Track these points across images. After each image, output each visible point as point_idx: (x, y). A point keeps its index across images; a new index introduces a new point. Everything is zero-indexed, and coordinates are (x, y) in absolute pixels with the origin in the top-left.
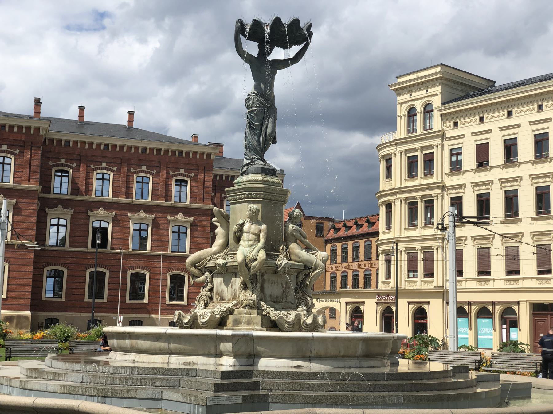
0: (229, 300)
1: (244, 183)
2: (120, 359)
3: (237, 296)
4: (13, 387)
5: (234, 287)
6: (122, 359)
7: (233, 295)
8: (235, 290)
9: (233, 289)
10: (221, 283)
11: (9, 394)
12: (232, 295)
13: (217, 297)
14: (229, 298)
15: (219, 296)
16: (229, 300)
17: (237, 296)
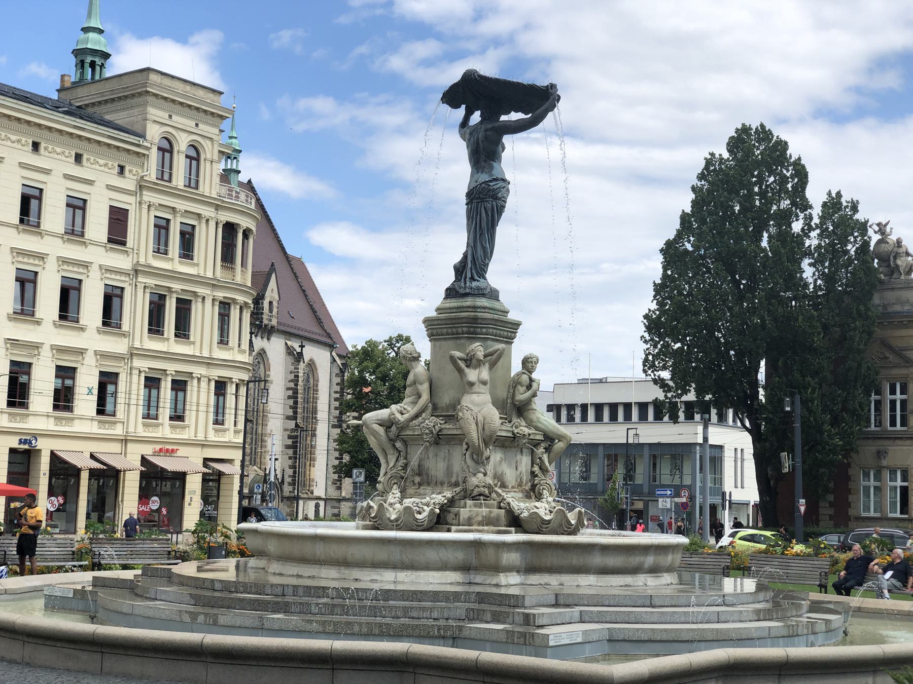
0: (513, 487)
1: (500, 313)
2: (657, 584)
3: (524, 483)
4: (834, 630)
5: (520, 469)
6: (660, 583)
7: (519, 480)
8: (521, 473)
9: (519, 472)
10: (501, 462)
11: (812, 645)
12: (517, 480)
13: (496, 482)
14: (514, 484)
15: (498, 481)
16: (513, 487)
17: (524, 483)
